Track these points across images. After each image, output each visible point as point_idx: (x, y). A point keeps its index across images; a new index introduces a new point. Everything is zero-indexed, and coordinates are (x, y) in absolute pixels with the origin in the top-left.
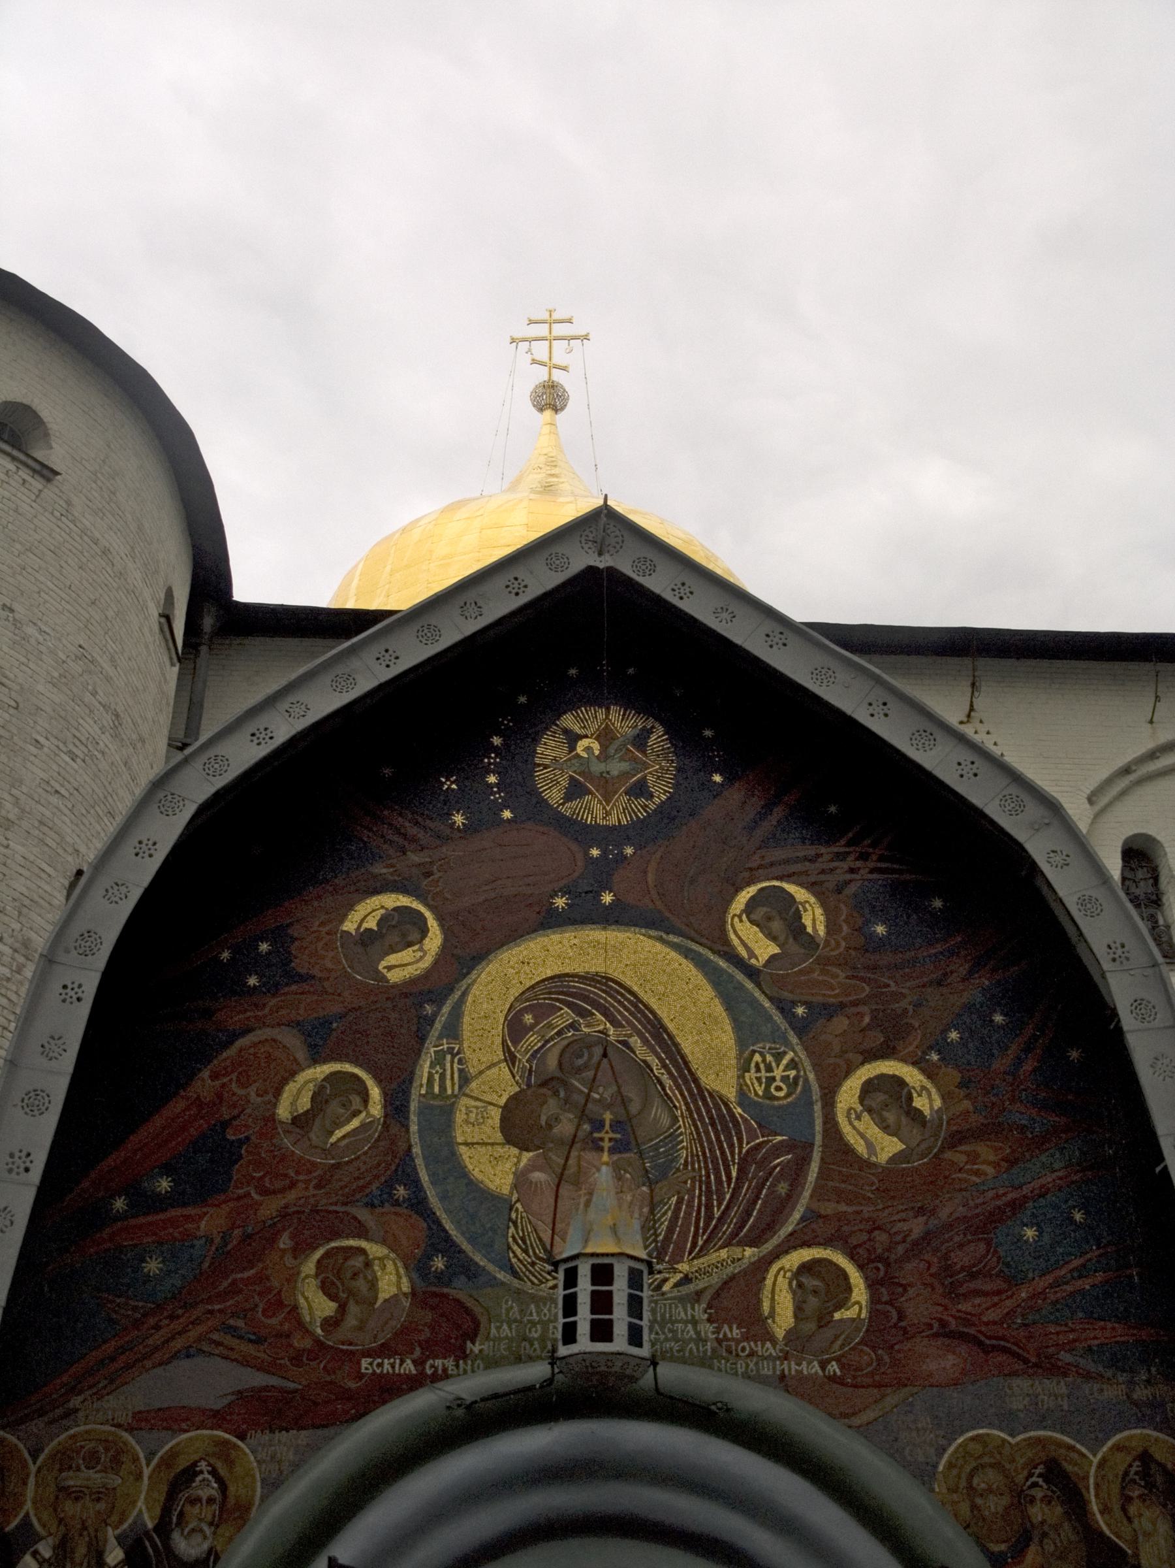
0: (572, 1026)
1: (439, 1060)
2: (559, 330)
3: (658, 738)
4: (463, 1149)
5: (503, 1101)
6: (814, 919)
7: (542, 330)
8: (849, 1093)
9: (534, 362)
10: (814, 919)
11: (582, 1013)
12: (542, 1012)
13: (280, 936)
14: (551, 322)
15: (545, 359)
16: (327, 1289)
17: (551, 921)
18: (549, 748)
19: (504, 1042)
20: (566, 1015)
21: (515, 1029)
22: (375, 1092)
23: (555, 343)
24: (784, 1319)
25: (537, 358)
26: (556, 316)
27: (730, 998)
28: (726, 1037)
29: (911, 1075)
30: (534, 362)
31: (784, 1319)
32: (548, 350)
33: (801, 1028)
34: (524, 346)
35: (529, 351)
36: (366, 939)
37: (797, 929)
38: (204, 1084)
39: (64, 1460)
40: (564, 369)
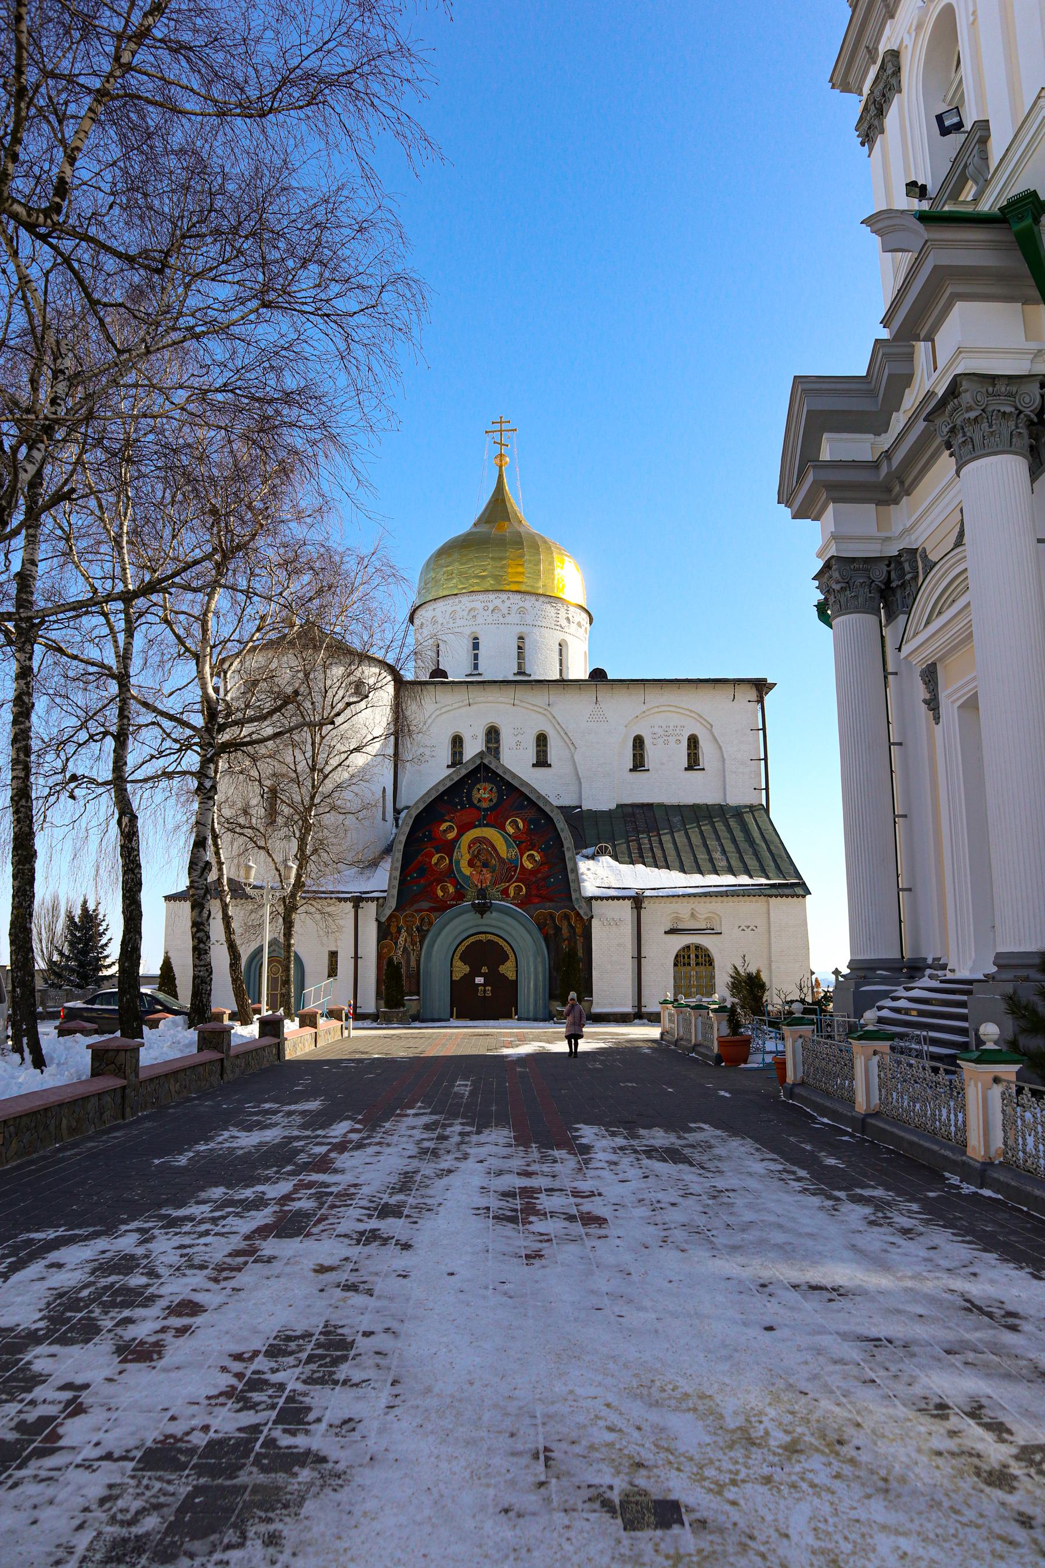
2: (505, 426)
3: (494, 790)
6: (521, 825)
7: (497, 427)
8: (525, 857)
10: (521, 825)
12: (474, 844)
13: (430, 832)
14: (501, 422)
17: (476, 827)
18: (475, 792)
21: (470, 847)
24: (512, 895)
27: (506, 841)
28: (505, 848)
29: (535, 854)
31: (512, 895)
33: (518, 846)
36: (444, 831)
37: (518, 827)
38: (419, 857)
39: (406, 916)
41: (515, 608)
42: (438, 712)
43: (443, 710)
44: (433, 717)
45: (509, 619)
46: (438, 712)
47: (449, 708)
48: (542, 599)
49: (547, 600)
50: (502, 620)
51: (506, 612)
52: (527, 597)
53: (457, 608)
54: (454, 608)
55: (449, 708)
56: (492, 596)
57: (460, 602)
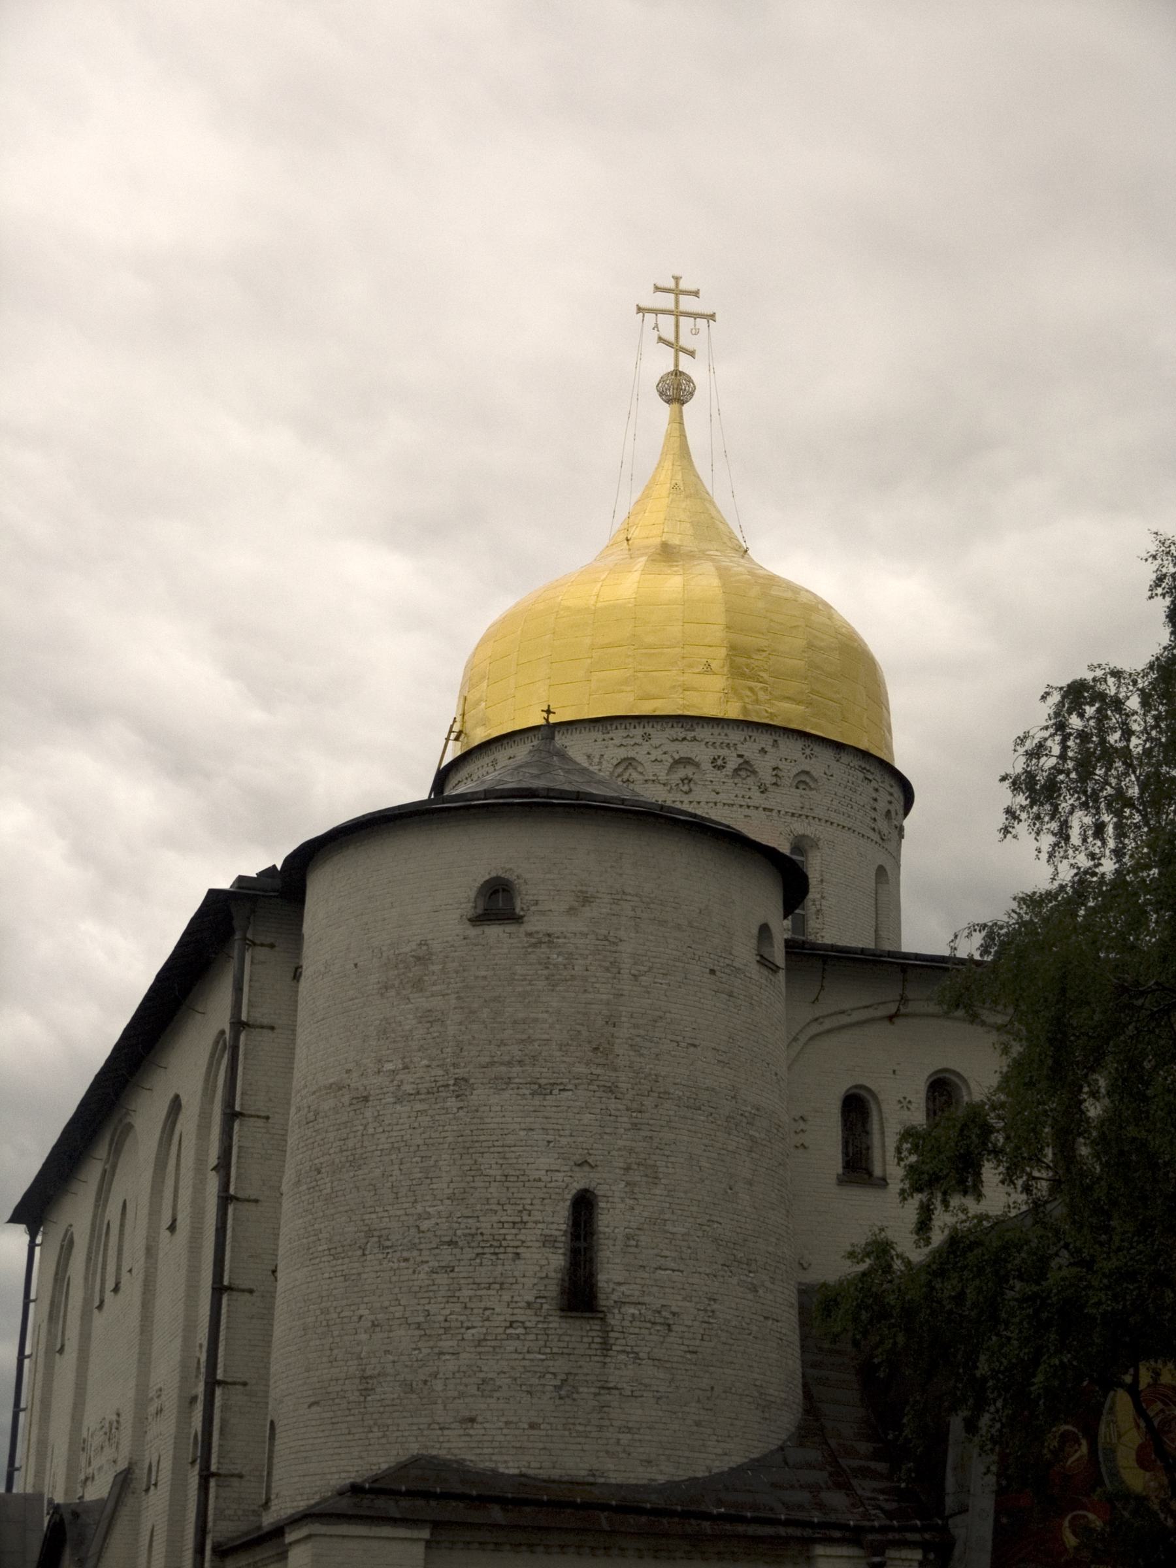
0: (1162, 1411)
1: (1108, 1426)
2: (687, 303)
4: (1122, 1471)
5: (1136, 1447)
7: (667, 301)
9: (661, 339)
11: (1166, 1404)
15: (672, 338)
16: (1075, 1533)
19: (1135, 1419)
20: (1160, 1405)
22: (1084, 1442)
23: (682, 319)
25: (664, 336)
26: (683, 285)
30: (661, 339)
32: (673, 328)
34: (650, 317)
35: (656, 327)
40: (692, 354)
41: (789, 771)
42: (815, 1029)
43: (828, 1024)
44: (803, 1038)
45: (775, 799)
46: (815, 1029)
47: (845, 1019)
48: (845, 758)
49: (856, 762)
50: (757, 798)
51: (767, 778)
52: (817, 749)
53: (640, 754)
54: (622, 753)
55: (845, 1019)
56: (735, 736)
57: (647, 737)
